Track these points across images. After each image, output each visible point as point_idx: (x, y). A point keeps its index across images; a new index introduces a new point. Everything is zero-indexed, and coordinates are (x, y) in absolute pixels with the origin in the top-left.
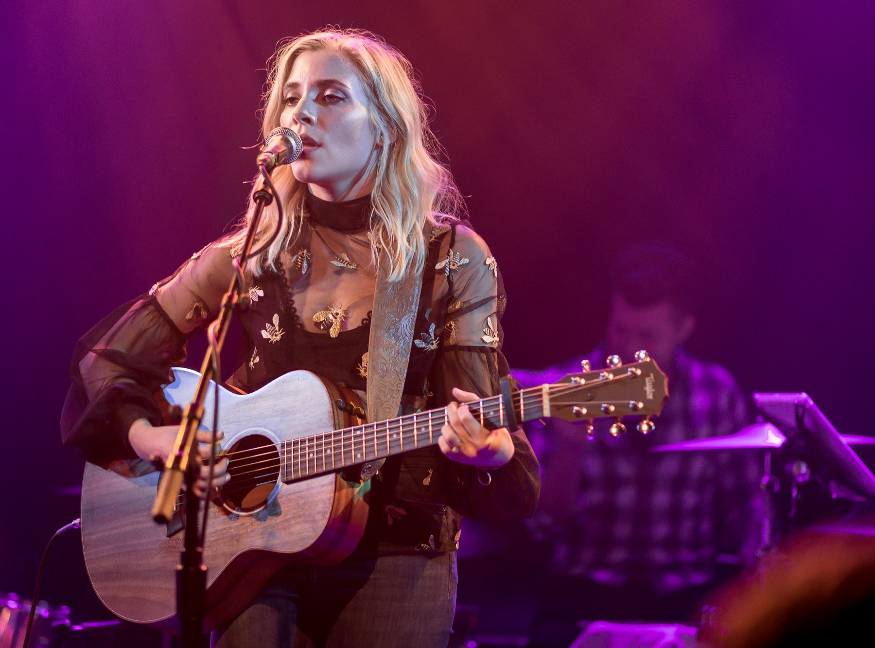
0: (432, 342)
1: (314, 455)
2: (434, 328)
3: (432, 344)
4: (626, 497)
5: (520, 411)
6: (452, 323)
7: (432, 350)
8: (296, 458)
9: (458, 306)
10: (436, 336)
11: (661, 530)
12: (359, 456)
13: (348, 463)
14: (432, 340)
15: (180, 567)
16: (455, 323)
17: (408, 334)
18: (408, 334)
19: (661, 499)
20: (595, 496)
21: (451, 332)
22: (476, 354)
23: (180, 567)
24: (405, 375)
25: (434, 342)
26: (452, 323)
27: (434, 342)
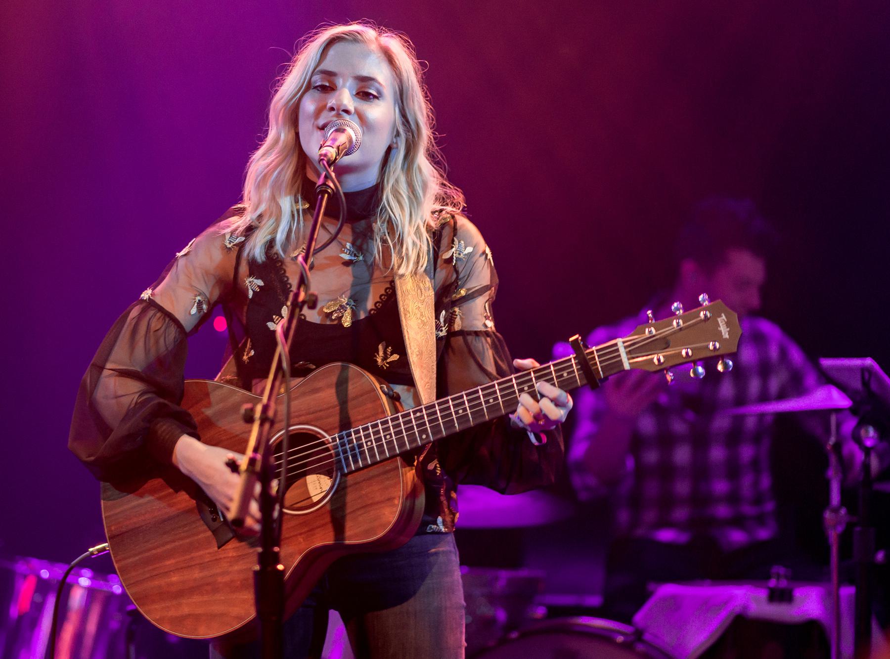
0: (441, 329)
1: (372, 444)
2: (444, 315)
3: (442, 331)
4: (682, 455)
5: (598, 368)
6: (457, 309)
7: (442, 337)
8: (353, 449)
9: (463, 292)
10: (445, 322)
11: (720, 487)
12: (424, 436)
13: (414, 445)
14: (442, 327)
15: (257, 568)
16: (459, 309)
17: (430, 317)
18: (430, 317)
19: (717, 454)
20: (651, 457)
21: (456, 318)
22: (483, 339)
23: (257, 568)
24: (435, 356)
25: (443, 328)
26: (457, 309)
27: (443, 328)
